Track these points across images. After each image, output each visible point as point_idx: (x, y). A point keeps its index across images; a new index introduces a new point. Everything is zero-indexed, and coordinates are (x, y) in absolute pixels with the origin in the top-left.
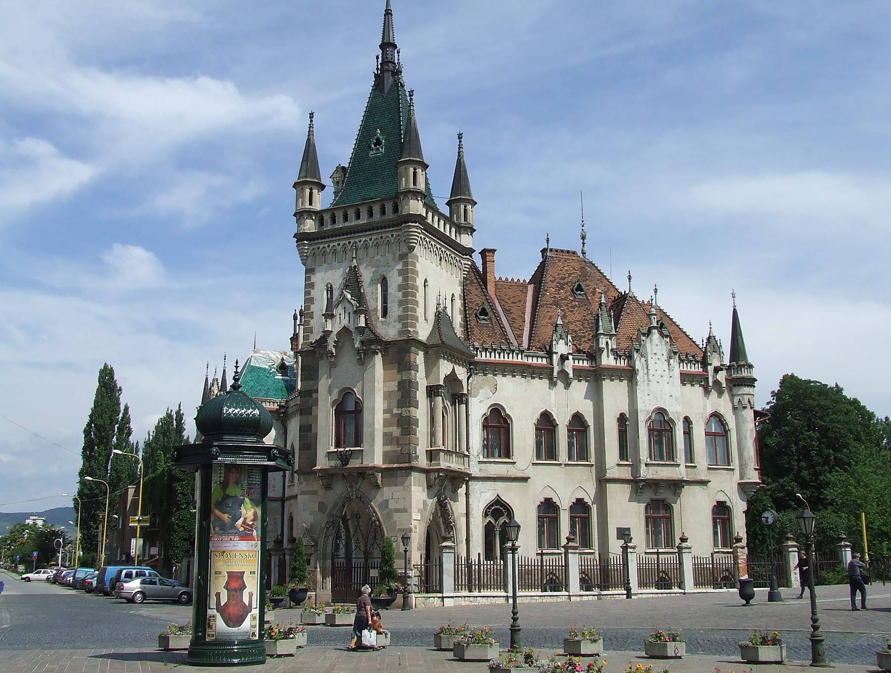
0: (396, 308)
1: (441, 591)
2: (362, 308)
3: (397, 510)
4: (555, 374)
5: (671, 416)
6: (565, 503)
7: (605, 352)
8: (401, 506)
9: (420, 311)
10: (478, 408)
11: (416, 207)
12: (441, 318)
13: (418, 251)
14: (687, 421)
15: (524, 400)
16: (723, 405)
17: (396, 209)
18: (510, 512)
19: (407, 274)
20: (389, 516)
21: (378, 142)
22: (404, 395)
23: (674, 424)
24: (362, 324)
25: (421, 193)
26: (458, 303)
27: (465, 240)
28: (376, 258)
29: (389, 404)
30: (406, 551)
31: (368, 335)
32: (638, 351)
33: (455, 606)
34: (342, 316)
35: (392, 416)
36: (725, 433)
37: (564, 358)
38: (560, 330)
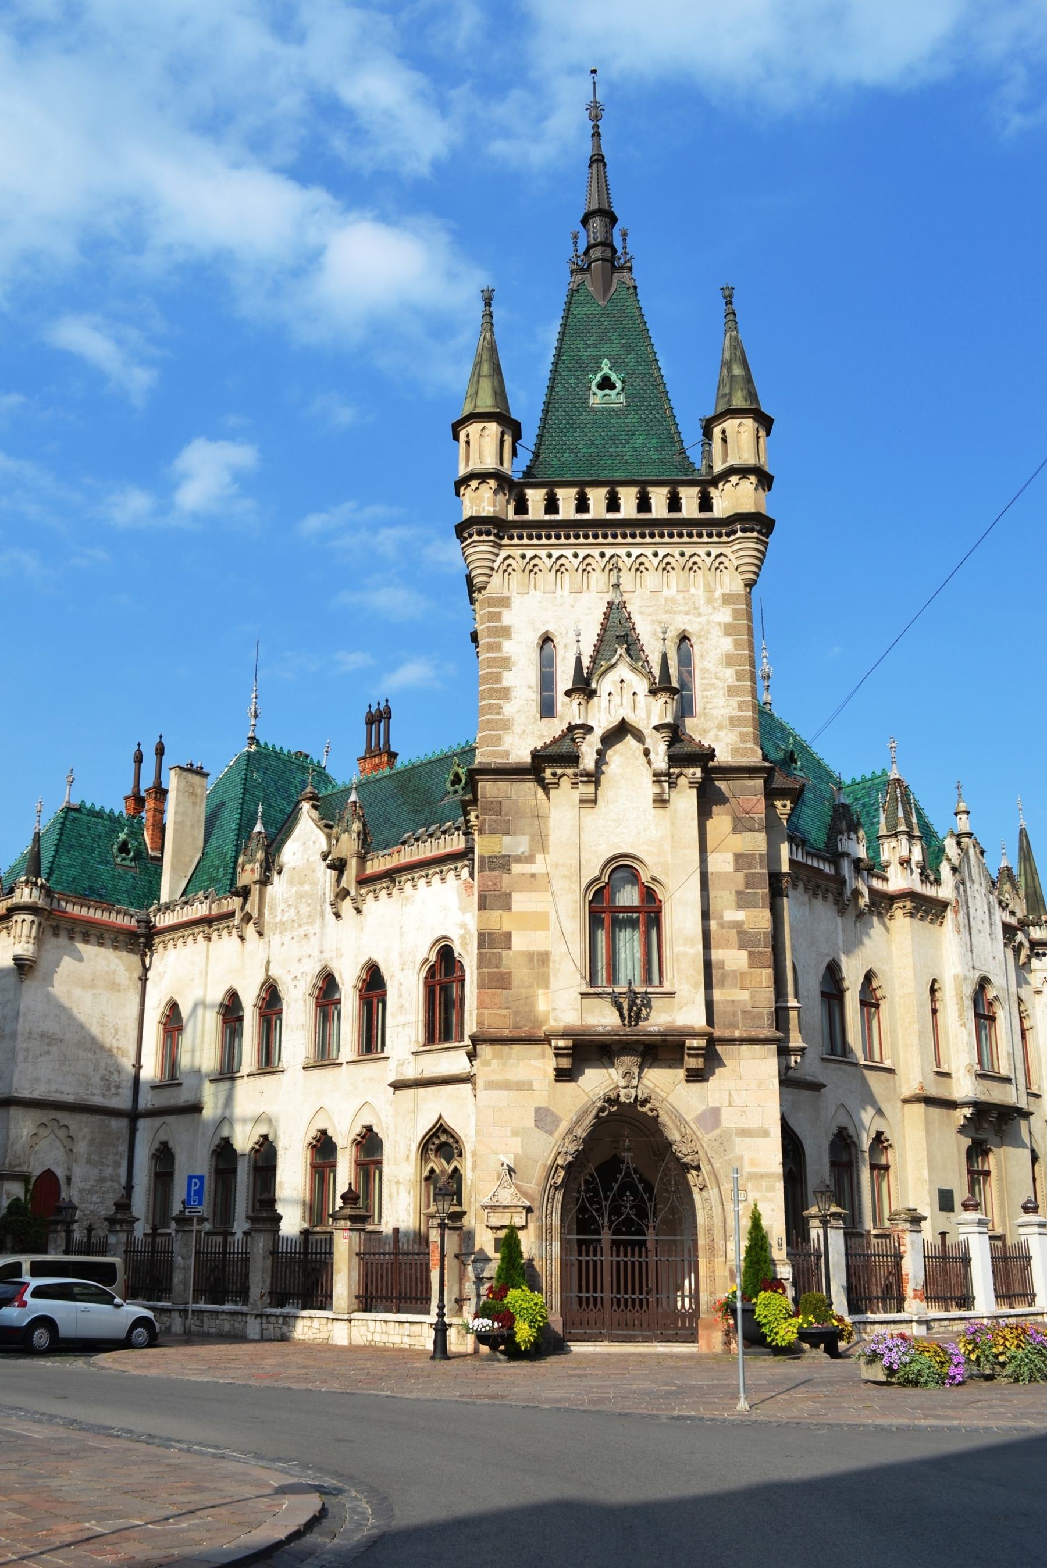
3: (744, 1133)
8: (753, 1122)
20: (724, 1142)
28: (666, 592)
34: (616, 699)
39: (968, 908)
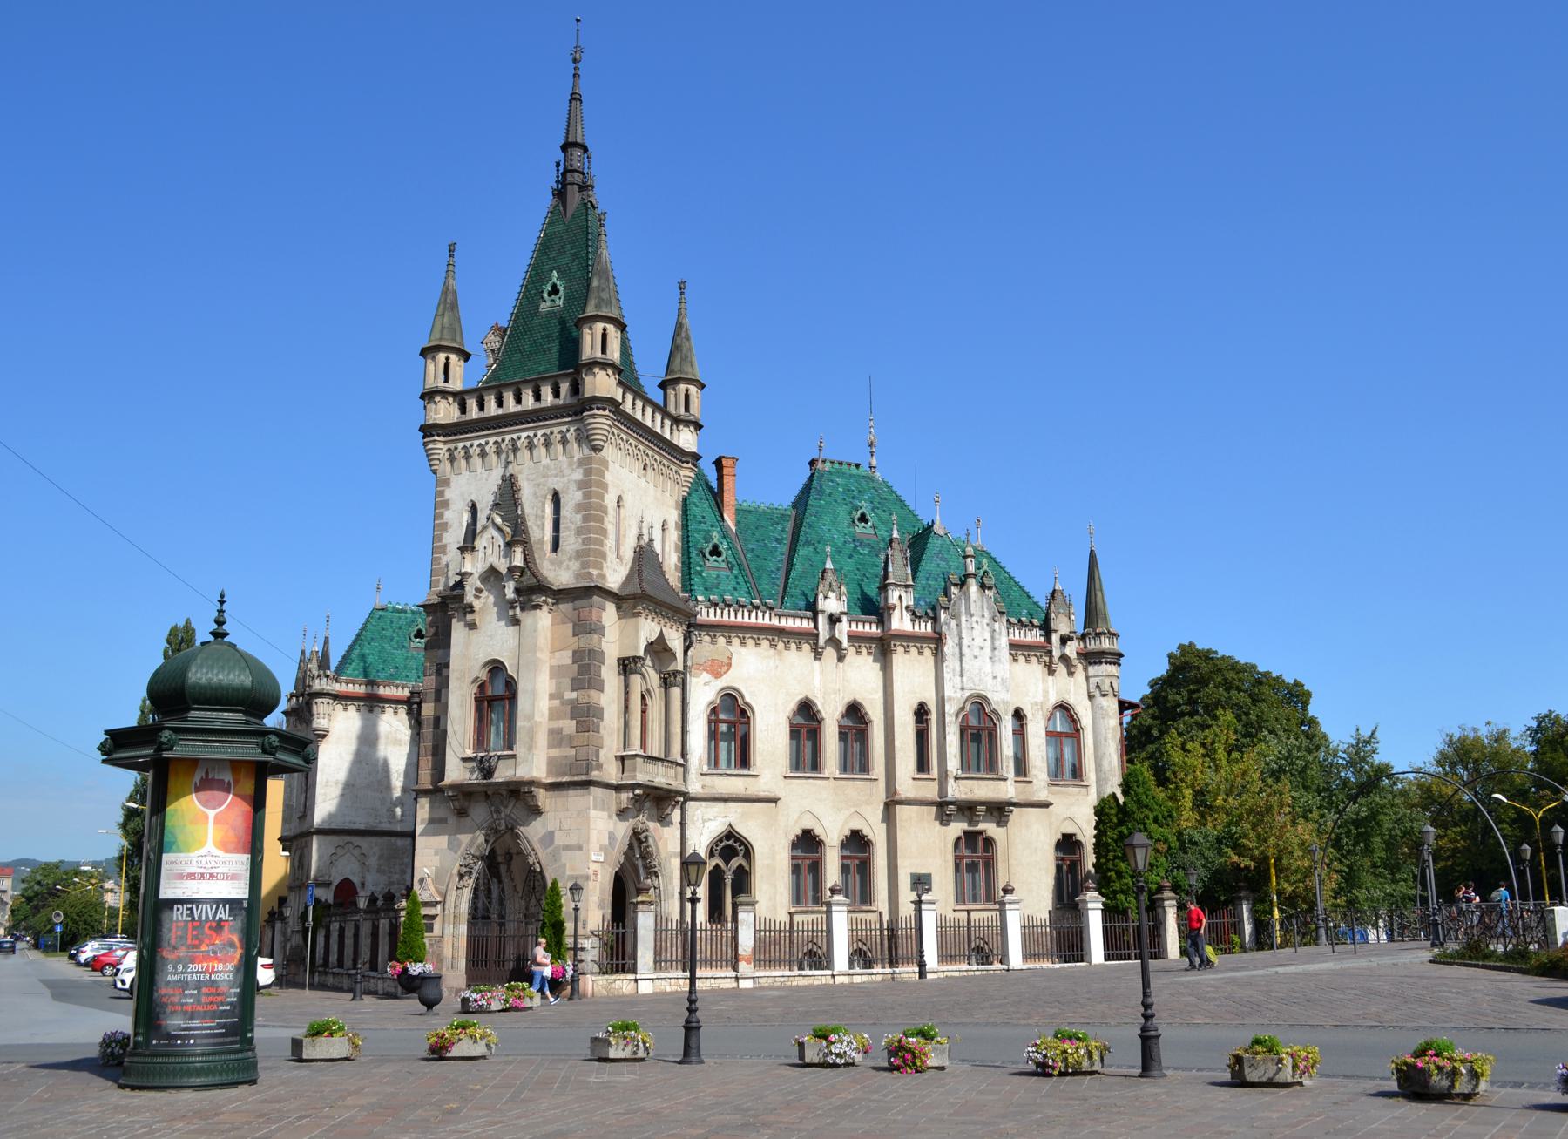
0: (572, 539)
1: (635, 972)
2: (517, 536)
4: (821, 642)
5: (994, 706)
6: (832, 834)
7: (896, 613)
8: (573, 841)
9: (610, 543)
10: (703, 693)
11: (602, 384)
12: (645, 556)
13: (609, 452)
14: (1018, 715)
15: (772, 680)
16: (1073, 688)
17: (576, 389)
18: (748, 853)
19: (591, 485)
20: (555, 857)
21: (555, 291)
22: (584, 669)
23: (999, 718)
24: (518, 561)
25: (612, 366)
26: (674, 535)
27: (686, 439)
29: (558, 686)
30: (576, 909)
31: (528, 580)
32: (946, 608)
33: (655, 994)
34: (489, 551)
35: (562, 703)
36: (1075, 732)
37: (834, 620)
38: (830, 577)
39: (961, 638)
